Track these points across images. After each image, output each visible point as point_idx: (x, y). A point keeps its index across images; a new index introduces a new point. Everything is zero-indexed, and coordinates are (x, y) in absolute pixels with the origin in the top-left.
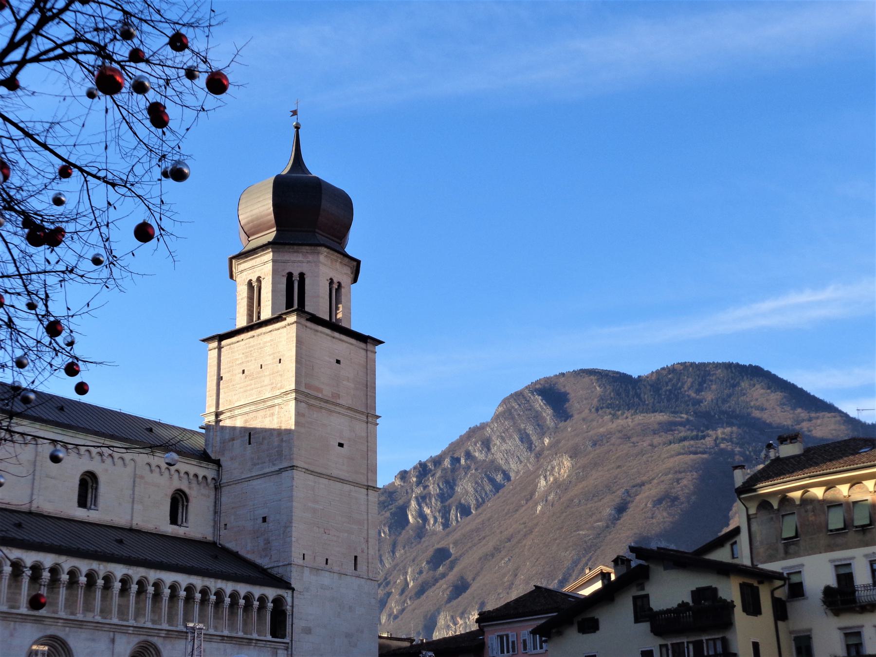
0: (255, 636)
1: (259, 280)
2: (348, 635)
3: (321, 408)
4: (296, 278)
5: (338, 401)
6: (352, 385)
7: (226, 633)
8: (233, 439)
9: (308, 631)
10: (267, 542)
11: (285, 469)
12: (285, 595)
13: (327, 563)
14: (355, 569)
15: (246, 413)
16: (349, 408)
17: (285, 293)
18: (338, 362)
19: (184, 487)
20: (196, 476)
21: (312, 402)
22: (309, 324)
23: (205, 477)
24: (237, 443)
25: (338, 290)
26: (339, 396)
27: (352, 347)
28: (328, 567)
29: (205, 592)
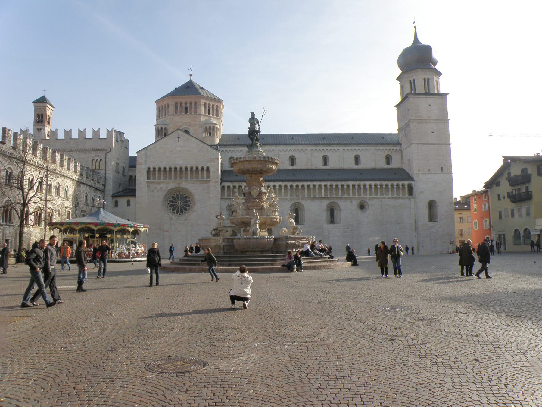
0: (401, 196)
1: (403, 85)
3: (423, 122)
4: (412, 81)
7: (390, 196)
8: (403, 136)
9: (422, 192)
11: (411, 144)
12: (412, 183)
13: (429, 171)
14: (442, 171)
15: (404, 128)
16: (435, 120)
18: (430, 105)
19: (390, 153)
20: (393, 149)
21: (419, 121)
22: (416, 96)
23: (396, 149)
25: (428, 82)
28: (430, 172)
29: (381, 185)
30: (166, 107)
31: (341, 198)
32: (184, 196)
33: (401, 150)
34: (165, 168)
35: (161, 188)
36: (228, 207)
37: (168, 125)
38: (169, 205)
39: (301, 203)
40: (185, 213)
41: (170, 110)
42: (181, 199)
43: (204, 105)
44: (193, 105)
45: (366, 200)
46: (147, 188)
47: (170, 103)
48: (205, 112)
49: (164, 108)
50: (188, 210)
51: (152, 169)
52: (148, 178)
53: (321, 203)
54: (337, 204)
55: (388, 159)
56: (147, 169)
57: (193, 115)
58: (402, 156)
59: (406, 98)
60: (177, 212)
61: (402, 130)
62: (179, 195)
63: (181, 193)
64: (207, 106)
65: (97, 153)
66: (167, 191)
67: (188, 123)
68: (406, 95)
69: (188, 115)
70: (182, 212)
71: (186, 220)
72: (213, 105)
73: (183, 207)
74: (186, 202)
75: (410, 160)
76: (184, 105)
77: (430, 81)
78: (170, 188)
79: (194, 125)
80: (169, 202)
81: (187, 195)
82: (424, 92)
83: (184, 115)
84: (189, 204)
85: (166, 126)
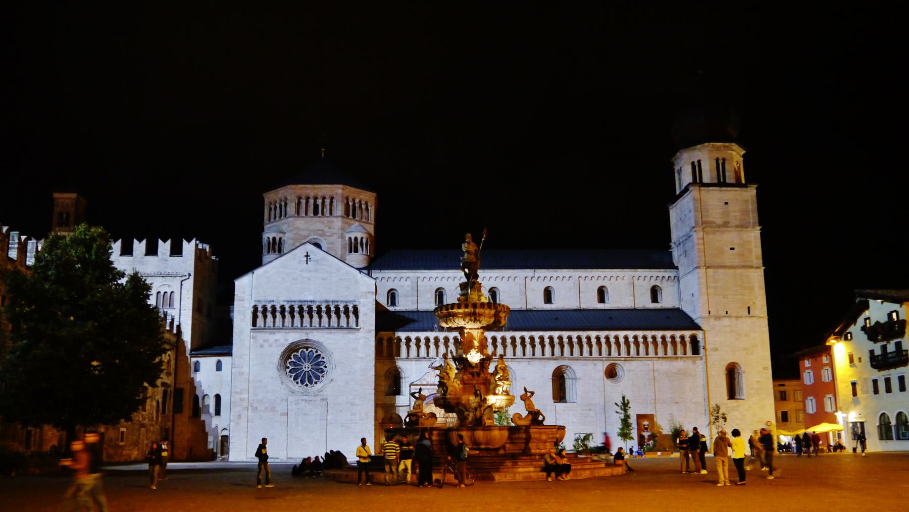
2: (745, 349)
4: (696, 164)
5: (728, 225)
6: (738, 214)
8: (681, 255)
10: (694, 307)
14: (749, 313)
15: (683, 242)
16: (737, 227)
17: (691, 174)
18: (726, 203)
19: (658, 283)
22: (702, 188)
23: (669, 277)
24: (682, 257)
25: (723, 164)
26: (728, 222)
27: (737, 192)
29: (645, 338)
30: (283, 204)
31: (577, 359)
32: (315, 355)
33: (677, 279)
34: (283, 308)
35: (276, 340)
36: (388, 374)
37: (284, 233)
38: (288, 370)
39: (511, 366)
40: (316, 383)
41: (288, 209)
42: (309, 359)
43: (346, 201)
44: (328, 201)
45: (619, 362)
46: (252, 340)
47: (289, 198)
48: (347, 214)
49: (278, 205)
50: (322, 379)
51: (260, 309)
52: (254, 324)
53: (544, 367)
54: (570, 368)
55: (655, 293)
56: (252, 309)
57: (328, 217)
58: (679, 288)
59: (686, 192)
60: (302, 382)
61: (679, 244)
62: (307, 352)
63: (309, 350)
64: (351, 204)
65: (166, 281)
66: (286, 346)
67: (319, 230)
68: (686, 187)
69: (320, 217)
70: (310, 381)
71: (317, 395)
72: (360, 202)
73: (313, 373)
74: (318, 364)
75: (693, 294)
76: (311, 201)
77: (726, 162)
78: (291, 341)
79: (329, 234)
80: (288, 365)
81: (319, 353)
82: (716, 181)
83: (312, 217)
84: (324, 368)
85: (281, 235)
